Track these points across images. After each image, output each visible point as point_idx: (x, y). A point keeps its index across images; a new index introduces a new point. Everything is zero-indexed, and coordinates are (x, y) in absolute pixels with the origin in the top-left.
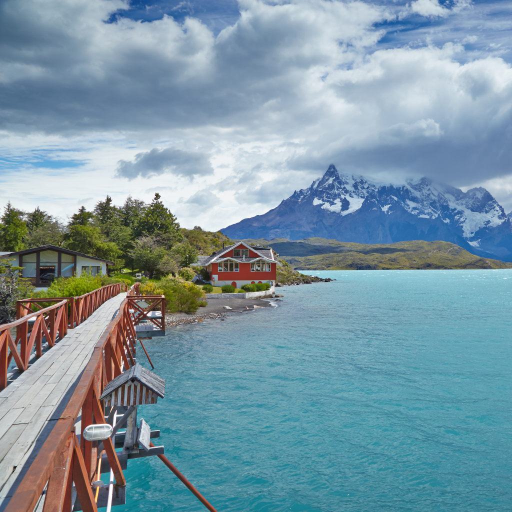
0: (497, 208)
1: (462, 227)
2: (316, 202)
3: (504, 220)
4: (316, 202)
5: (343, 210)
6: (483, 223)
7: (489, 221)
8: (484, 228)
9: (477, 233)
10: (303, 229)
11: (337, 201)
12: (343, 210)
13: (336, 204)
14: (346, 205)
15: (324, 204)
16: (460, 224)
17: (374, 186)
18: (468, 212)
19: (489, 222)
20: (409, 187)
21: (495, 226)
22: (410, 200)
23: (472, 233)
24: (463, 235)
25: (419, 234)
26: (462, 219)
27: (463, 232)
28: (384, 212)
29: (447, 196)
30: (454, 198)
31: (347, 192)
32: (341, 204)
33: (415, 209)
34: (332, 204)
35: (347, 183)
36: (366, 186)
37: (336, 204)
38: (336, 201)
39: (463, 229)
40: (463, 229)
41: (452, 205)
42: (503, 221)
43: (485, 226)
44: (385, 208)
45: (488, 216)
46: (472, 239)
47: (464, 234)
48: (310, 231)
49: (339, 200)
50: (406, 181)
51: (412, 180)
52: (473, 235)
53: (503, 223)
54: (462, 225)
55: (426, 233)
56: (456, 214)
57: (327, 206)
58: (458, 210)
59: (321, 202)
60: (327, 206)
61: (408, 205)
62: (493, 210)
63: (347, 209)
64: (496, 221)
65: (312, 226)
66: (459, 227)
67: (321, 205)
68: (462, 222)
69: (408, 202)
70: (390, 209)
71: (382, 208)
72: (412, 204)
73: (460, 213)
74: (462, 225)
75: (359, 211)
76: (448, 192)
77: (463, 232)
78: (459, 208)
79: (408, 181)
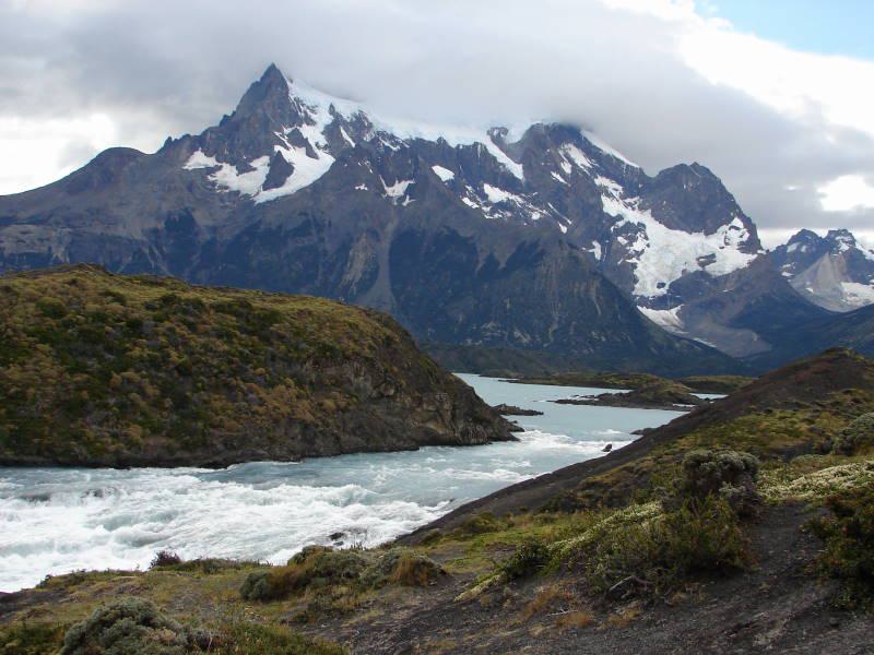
0: (737, 222)
1: (634, 266)
2: (199, 160)
3: (756, 256)
4: (199, 160)
5: (266, 186)
6: (694, 261)
7: (713, 256)
8: (696, 272)
9: (676, 287)
10: (121, 231)
11: (262, 165)
12: (266, 186)
13: (255, 169)
14: (280, 171)
15: (220, 168)
16: (630, 257)
17: (392, 137)
18: (655, 229)
19: (711, 258)
20: (494, 150)
21: (728, 269)
22: (494, 184)
23: (661, 285)
24: (633, 289)
25: (480, 266)
26: (638, 245)
27: (636, 281)
28: (389, 198)
29: (600, 181)
30: (620, 188)
31: (298, 141)
32: (267, 170)
33: (501, 206)
34: (244, 168)
35: (311, 122)
36: (367, 138)
37: (255, 169)
38: (254, 164)
39: (635, 272)
40: (635, 272)
41: (612, 207)
42: (753, 257)
43: (700, 269)
44: (398, 189)
45: (712, 243)
46: (659, 303)
47: (637, 286)
48: (138, 236)
49: (266, 159)
50: (488, 133)
51: (505, 131)
52: (663, 291)
53: (752, 264)
54: (634, 260)
55: (503, 265)
56: (619, 232)
57: (228, 176)
58: (626, 220)
59: (211, 162)
60: (228, 176)
61: (485, 196)
62: (725, 228)
63: (279, 184)
64: (732, 261)
65: (152, 224)
66: (625, 265)
67: (211, 171)
68: (638, 254)
69: (487, 188)
70: (409, 191)
71: (390, 191)
72: (496, 194)
73: (633, 230)
74: (634, 260)
75: (316, 188)
76: (607, 175)
77: (636, 281)
78: (633, 216)
79: (495, 133)
